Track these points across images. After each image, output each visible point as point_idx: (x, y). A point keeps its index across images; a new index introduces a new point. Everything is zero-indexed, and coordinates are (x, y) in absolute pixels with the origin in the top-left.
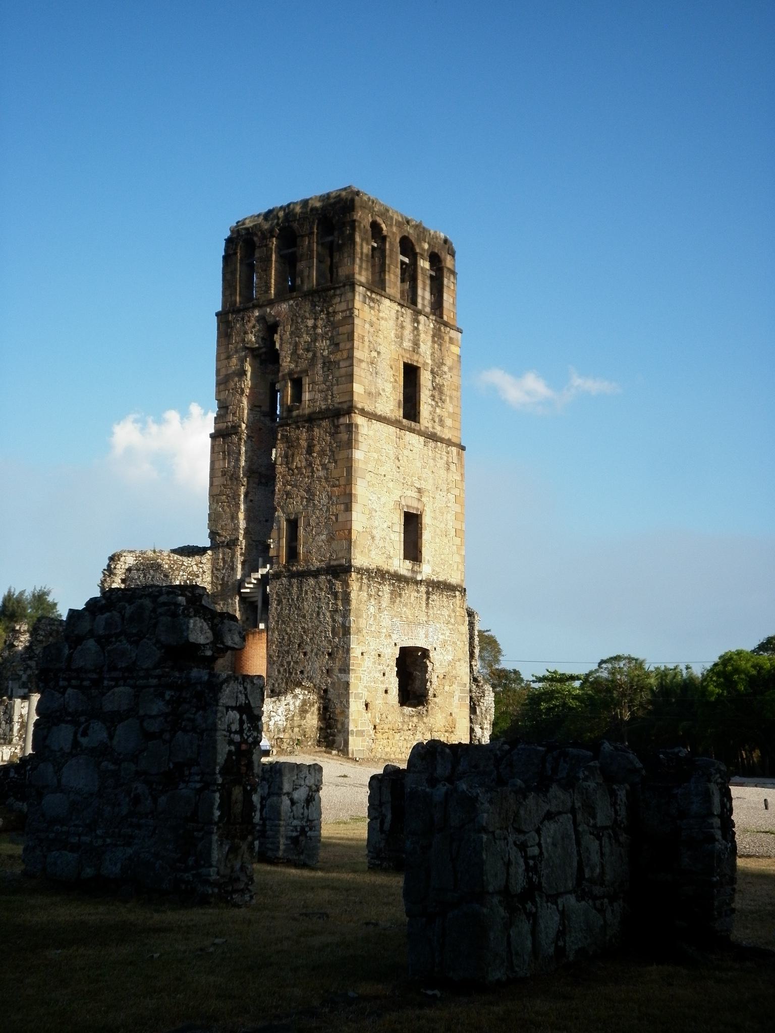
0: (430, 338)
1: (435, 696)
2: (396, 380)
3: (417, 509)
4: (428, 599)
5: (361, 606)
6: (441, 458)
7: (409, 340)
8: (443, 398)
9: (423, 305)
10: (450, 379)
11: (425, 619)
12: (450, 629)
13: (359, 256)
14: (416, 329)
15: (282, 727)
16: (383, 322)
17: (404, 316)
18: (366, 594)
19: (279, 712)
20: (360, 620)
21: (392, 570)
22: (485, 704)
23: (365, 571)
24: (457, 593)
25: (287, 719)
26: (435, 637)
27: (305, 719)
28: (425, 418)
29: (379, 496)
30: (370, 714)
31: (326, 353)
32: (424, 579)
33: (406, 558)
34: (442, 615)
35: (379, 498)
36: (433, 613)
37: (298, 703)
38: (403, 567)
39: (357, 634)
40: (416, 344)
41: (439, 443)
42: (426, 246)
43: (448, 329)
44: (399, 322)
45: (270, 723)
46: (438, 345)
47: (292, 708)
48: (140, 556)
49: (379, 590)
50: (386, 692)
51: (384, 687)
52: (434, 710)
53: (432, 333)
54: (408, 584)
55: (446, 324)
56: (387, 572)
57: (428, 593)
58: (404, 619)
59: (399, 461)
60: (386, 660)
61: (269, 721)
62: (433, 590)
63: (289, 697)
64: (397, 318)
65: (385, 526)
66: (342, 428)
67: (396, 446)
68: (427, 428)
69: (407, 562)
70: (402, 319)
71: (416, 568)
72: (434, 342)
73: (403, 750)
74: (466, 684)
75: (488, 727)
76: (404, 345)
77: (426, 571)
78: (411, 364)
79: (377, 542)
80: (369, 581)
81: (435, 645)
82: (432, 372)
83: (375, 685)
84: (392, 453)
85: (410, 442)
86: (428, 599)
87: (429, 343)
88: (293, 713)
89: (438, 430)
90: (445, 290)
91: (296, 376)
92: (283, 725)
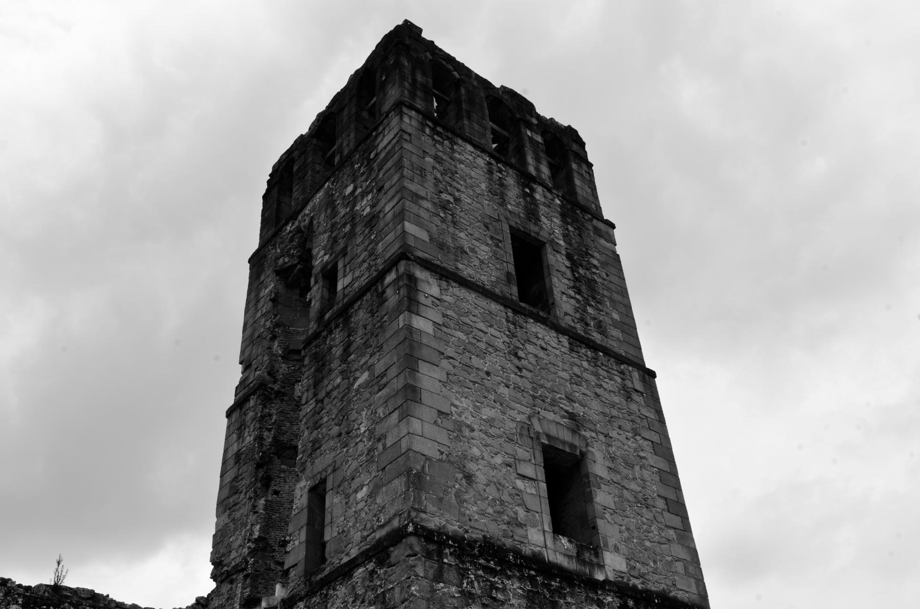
3: (572, 446)
14: (531, 196)
21: (527, 550)
23: (449, 538)
31: (368, 209)
33: (558, 529)
40: (532, 213)
41: (601, 354)
46: (574, 228)
54: (572, 585)
55: (585, 210)
56: (517, 553)
59: (519, 358)
64: (490, 172)
65: (498, 460)
66: (389, 292)
67: (507, 333)
69: (564, 541)
71: (587, 556)
80: (463, 562)
82: (569, 257)
85: (540, 336)
87: (557, 221)
89: (597, 337)
90: (575, 174)
91: (329, 266)
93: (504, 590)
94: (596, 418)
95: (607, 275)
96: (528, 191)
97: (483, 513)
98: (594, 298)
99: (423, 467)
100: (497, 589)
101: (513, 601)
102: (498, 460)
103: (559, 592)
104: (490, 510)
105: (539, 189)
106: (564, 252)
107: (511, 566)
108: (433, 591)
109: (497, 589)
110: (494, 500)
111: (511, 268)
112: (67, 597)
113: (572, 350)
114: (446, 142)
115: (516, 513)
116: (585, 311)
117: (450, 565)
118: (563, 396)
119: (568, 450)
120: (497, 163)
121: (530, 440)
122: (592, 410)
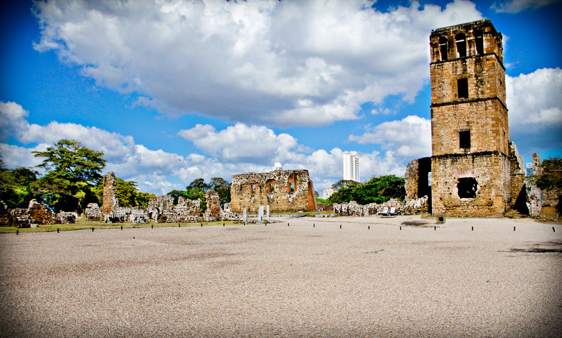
0: (474, 64)
1: (479, 193)
2: (453, 88)
3: (467, 129)
4: (474, 159)
6: (482, 107)
7: (460, 71)
9: (470, 54)
11: (472, 167)
12: (488, 169)
13: (433, 54)
14: (465, 64)
15: (419, 207)
16: (444, 71)
18: (438, 164)
20: (436, 173)
21: (453, 153)
22: (531, 193)
24: (492, 155)
26: (478, 173)
28: (472, 95)
30: (442, 202)
34: (482, 164)
36: (477, 165)
37: (426, 199)
38: (461, 151)
40: (465, 70)
42: (472, 31)
43: (485, 56)
44: (455, 66)
47: (423, 201)
49: (445, 161)
51: (449, 192)
52: (479, 199)
53: (474, 62)
57: (473, 158)
60: (450, 184)
62: (476, 156)
63: (422, 198)
64: (453, 66)
65: (449, 139)
68: (474, 98)
69: (462, 149)
71: (467, 150)
72: (476, 65)
73: (462, 212)
74: (499, 188)
75: (535, 202)
77: (473, 150)
78: (462, 79)
81: (478, 175)
84: (451, 113)
87: (473, 67)
89: (481, 96)
96: (464, 63)
97: (445, 150)
98: (482, 84)
101: (448, 162)
102: (449, 139)
103: (459, 159)
105: (467, 60)
106: (474, 76)
107: (448, 157)
111: (457, 93)
113: (471, 105)
114: (441, 67)
116: (478, 90)
119: (465, 130)
122: (473, 118)
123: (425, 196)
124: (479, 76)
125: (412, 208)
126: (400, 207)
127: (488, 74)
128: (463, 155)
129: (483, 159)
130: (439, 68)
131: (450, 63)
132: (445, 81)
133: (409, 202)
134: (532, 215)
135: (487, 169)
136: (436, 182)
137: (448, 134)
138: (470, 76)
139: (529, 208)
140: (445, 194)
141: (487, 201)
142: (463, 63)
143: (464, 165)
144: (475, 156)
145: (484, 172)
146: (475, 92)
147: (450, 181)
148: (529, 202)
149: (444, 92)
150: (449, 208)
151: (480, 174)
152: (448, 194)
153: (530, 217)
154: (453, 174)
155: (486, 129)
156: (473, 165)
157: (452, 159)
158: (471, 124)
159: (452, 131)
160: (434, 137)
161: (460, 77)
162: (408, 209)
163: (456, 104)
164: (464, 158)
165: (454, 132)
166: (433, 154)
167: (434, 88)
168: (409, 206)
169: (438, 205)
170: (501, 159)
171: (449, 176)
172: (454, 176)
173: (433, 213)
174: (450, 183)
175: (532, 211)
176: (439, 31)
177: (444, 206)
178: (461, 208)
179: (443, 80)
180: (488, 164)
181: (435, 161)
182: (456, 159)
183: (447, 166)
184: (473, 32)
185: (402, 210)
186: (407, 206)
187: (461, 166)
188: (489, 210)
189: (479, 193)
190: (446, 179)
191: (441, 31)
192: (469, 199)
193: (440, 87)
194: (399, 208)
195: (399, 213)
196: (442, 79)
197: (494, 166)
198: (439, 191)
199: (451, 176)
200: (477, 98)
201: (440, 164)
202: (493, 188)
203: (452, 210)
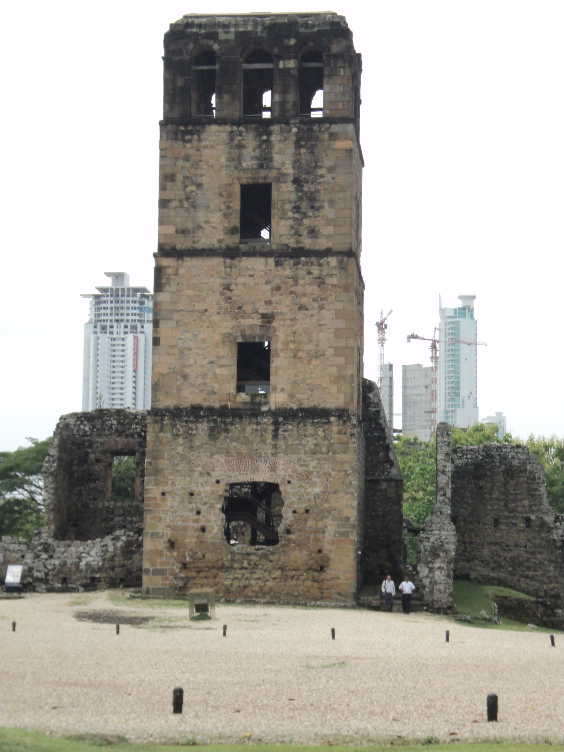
0: (293, 145)
1: (288, 532)
2: (228, 207)
5: (161, 447)
8: (317, 205)
10: (331, 181)
11: (270, 451)
14: (268, 141)
15: (96, 567)
16: (206, 152)
17: (244, 134)
18: (169, 435)
19: (93, 553)
22: (432, 539)
24: (332, 419)
25: (104, 560)
26: (290, 470)
27: (130, 559)
28: (281, 236)
29: (196, 333)
30: (175, 554)
32: (273, 408)
34: (301, 445)
35: (195, 336)
36: (287, 446)
37: (119, 544)
39: (155, 474)
41: (303, 258)
42: (293, 42)
43: (327, 125)
44: (236, 142)
45: (81, 564)
46: (308, 149)
47: (111, 549)
48: (81, 417)
50: (203, 529)
51: (199, 525)
53: (294, 138)
54: (241, 417)
57: (276, 424)
58: (234, 454)
59: (231, 291)
60: (202, 499)
61: (79, 562)
62: (286, 418)
63: (108, 540)
64: (232, 140)
65: (206, 362)
68: (287, 245)
70: (240, 138)
72: (298, 145)
73: (233, 589)
76: (244, 165)
79: (192, 380)
80: (174, 421)
81: (287, 478)
83: (183, 524)
84: (217, 282)
85: (250, 267)
86: (276, 431)
87: (290, 149)
88: (112, 554)
89: (307, 242)
92: (98, 565)
93: (197, 429)
94: (285, 310)
95: (333, 178)
96: (265, 138)
97: (192, 393)
98: (312, 207)
99: (159, 379)
100: (192, 430)
101: (201, 433)
103: (232, 424)
104: (197, 391)
105: (276, 128)
106: (292, 179)
107: (202, 417)
108: (157, 437)
109: (192, 430)
110: (200, 385)
111: (236, 222)
112: (106, 414)
114: (195, 137)
115: (213, 388)
117: (167, 424)
118: (263, 303)
120: (238, 128)
121: (229, 343)
123: (118, 533)
124: (307, 182)
125: (74, 569)
126: (35, 565)
127: (331, 181)
128: (247, 414)
129: (305, 430)
130: (190, 141)
131: (222, 128)
132: (205, 180)
133: (63, 549)
134: (432, 602)
135: (317, 461)
136: (161, 490)
137: (203, 346)
138: (281, 177)
139: (426, 582)
140: (185, 529)
141: (310, 555)
142: (260, 135)
143: (247, 442)
144: (281, 419)
145: (306, 469)
146: (292, 227)
147: (202, 489)
148: (427, 563)
149: (201, 216)
150: (194, 574)
151: (295, 474)
152: (196, 530)
153: (427, 610)
154: (213, 470)
155: (318, 341)
156: (275, 446)
157: (212, 424)
158: (275, 324)
159: (218, 338)
160: (162, 348)
161: (249, 175)
162: (60, 572)
163: (232, 258)
164: (250, 423)
165: (223, 342)
166: (153, 402)
167: (168, 201)
168: (64, 564)
169: (162, 563)
170: (356, 434)
171: (201, 474)
172: (216, 474)
173: (145, 586)
174: (203, 495)
175: (435, 592)
176: (192, 25)
177: (179, 565)
178: (231, 577)
179: (199, 181)
180: (316, 445)
181: (158, 427)
182: (226, 424)
183: (197, 443)
184: (295, 44)
185: (39, 575)
186: (57, 562)
187: (239, 446)
188: (316, 584)
189: (288, 532)
190: (191, 482)
191: (200, 26)
192: (257, 547)
193: (187, 199)
194: (31, 569)
195: (29, 584)
196: (195, 175)
197: (335, 453)
198: (168, 519)
199: (209, 474)
200: (295, 246)
201: (177, 436)
202: (330, 517)
203: (205, 581)
